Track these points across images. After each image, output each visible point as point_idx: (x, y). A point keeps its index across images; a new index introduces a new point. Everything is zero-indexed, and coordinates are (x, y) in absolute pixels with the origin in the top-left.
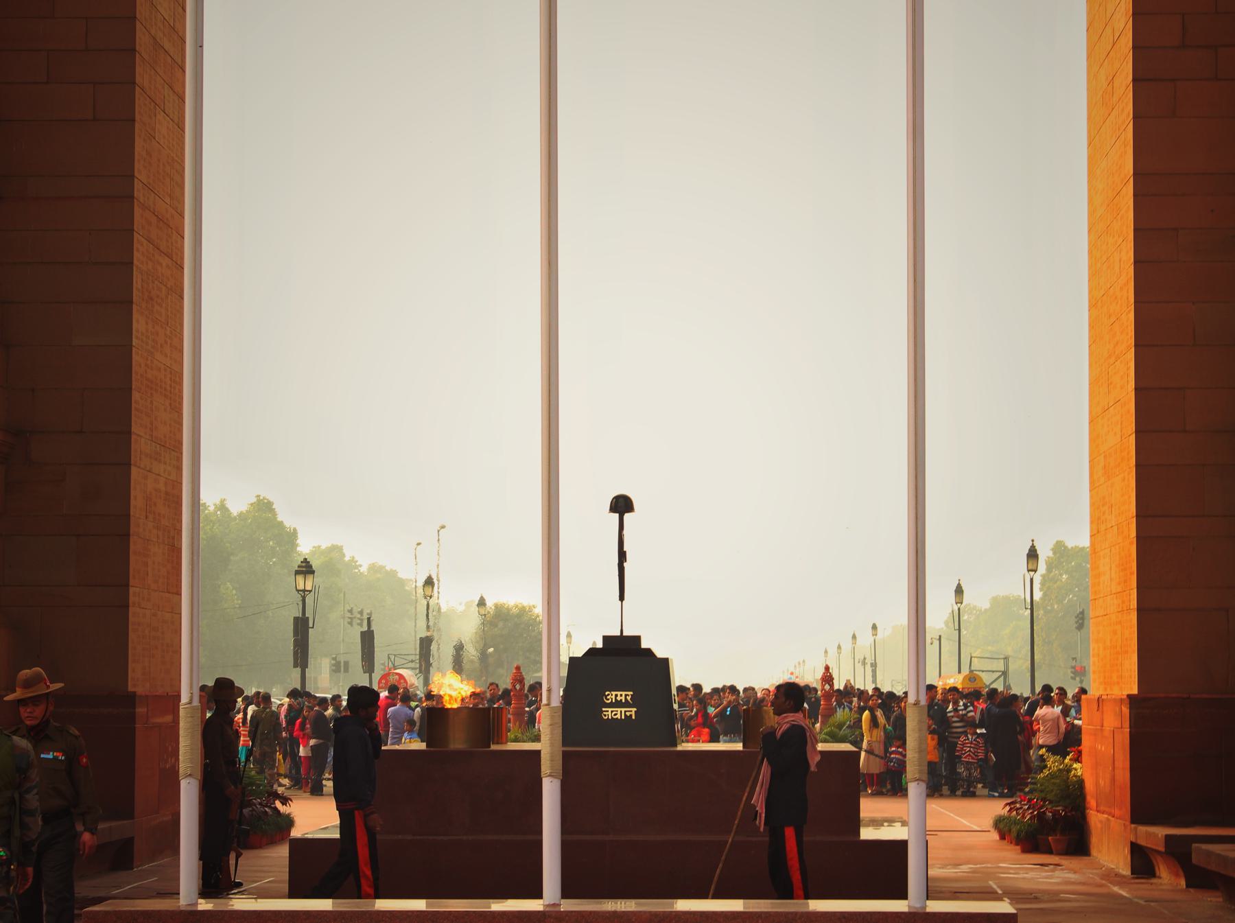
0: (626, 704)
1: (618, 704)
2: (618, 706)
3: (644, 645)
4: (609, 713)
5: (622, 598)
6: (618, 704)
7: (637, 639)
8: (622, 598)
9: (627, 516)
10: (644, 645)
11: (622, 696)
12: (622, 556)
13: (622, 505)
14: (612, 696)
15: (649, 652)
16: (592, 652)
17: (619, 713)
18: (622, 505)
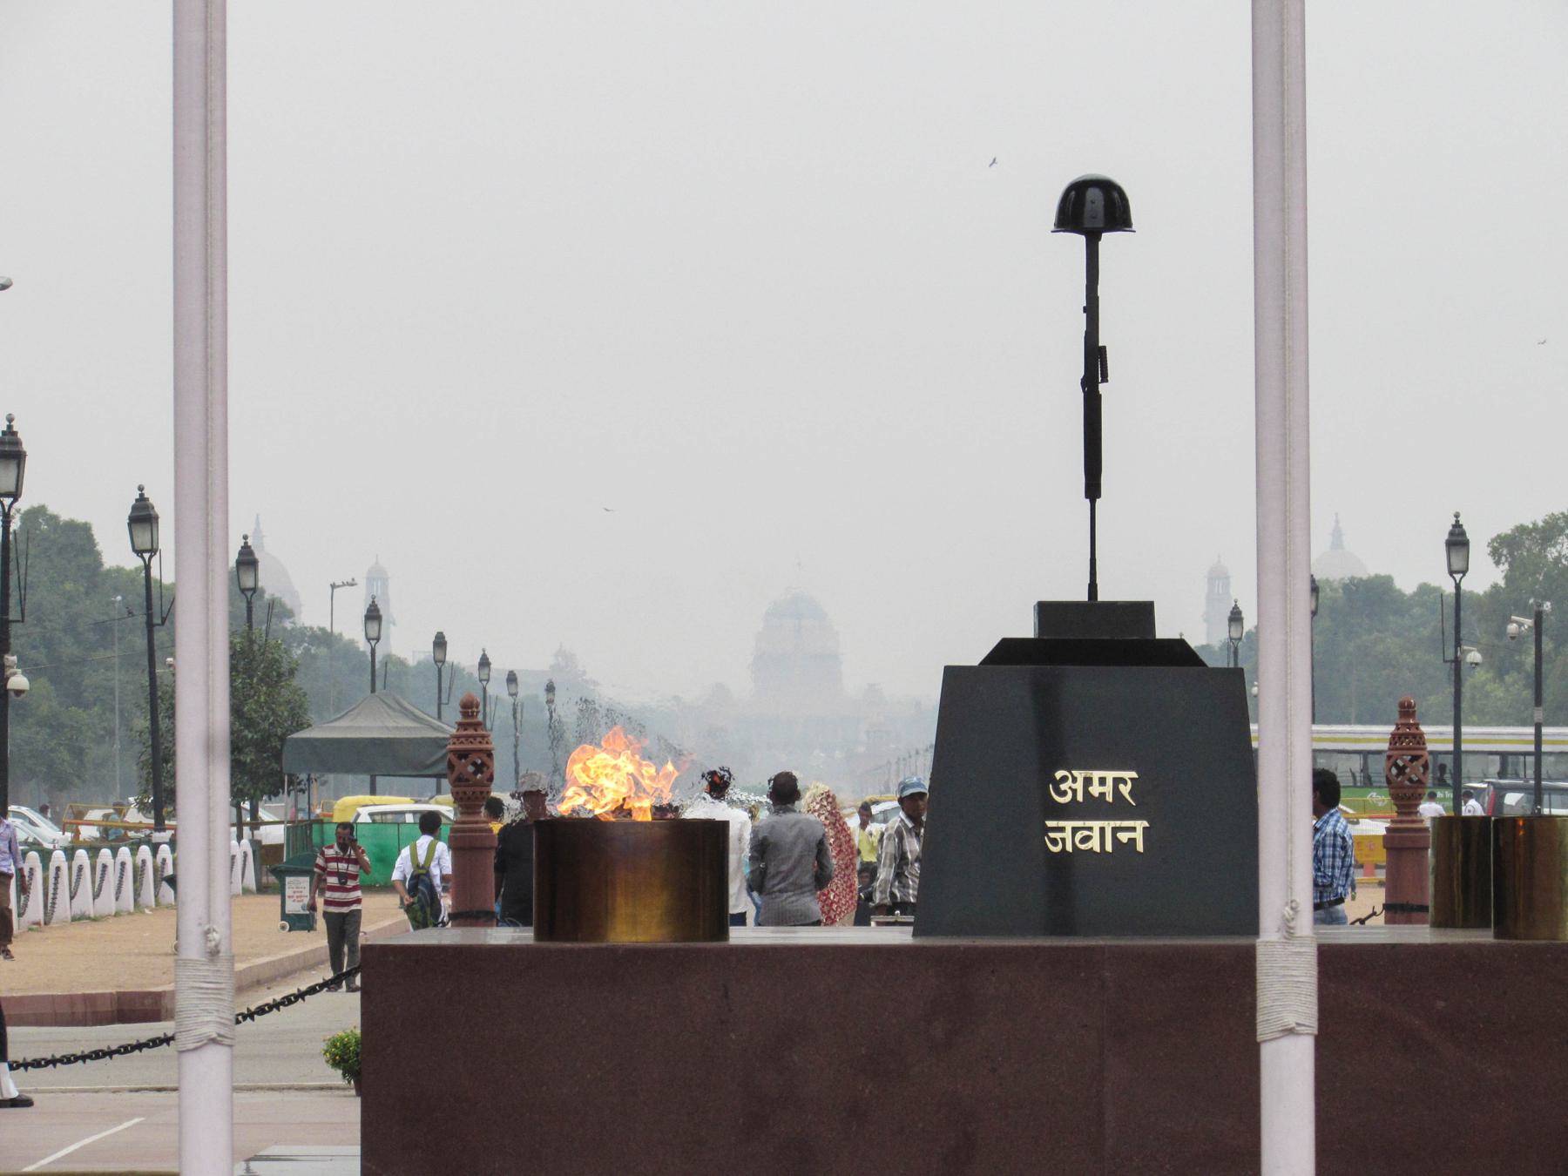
0: (1115, 809)
1: (1092, 808)
2: (1096, 813)
3: (1164, 630)
4: (1065, 835)
5: (1093, 490)
6: (1092, 808)
7: (1143, 611)
8: (1093, 490)
9: (1108, 240)
10: (1164, 630)
11: (1105, 781)
12: (1095, 358)
13: (1093, 209)
14: (1072, 784)
15: (1179, 652)
16: (1007, 652)
17: (1097, 835)
18: (1093, 209)
